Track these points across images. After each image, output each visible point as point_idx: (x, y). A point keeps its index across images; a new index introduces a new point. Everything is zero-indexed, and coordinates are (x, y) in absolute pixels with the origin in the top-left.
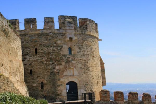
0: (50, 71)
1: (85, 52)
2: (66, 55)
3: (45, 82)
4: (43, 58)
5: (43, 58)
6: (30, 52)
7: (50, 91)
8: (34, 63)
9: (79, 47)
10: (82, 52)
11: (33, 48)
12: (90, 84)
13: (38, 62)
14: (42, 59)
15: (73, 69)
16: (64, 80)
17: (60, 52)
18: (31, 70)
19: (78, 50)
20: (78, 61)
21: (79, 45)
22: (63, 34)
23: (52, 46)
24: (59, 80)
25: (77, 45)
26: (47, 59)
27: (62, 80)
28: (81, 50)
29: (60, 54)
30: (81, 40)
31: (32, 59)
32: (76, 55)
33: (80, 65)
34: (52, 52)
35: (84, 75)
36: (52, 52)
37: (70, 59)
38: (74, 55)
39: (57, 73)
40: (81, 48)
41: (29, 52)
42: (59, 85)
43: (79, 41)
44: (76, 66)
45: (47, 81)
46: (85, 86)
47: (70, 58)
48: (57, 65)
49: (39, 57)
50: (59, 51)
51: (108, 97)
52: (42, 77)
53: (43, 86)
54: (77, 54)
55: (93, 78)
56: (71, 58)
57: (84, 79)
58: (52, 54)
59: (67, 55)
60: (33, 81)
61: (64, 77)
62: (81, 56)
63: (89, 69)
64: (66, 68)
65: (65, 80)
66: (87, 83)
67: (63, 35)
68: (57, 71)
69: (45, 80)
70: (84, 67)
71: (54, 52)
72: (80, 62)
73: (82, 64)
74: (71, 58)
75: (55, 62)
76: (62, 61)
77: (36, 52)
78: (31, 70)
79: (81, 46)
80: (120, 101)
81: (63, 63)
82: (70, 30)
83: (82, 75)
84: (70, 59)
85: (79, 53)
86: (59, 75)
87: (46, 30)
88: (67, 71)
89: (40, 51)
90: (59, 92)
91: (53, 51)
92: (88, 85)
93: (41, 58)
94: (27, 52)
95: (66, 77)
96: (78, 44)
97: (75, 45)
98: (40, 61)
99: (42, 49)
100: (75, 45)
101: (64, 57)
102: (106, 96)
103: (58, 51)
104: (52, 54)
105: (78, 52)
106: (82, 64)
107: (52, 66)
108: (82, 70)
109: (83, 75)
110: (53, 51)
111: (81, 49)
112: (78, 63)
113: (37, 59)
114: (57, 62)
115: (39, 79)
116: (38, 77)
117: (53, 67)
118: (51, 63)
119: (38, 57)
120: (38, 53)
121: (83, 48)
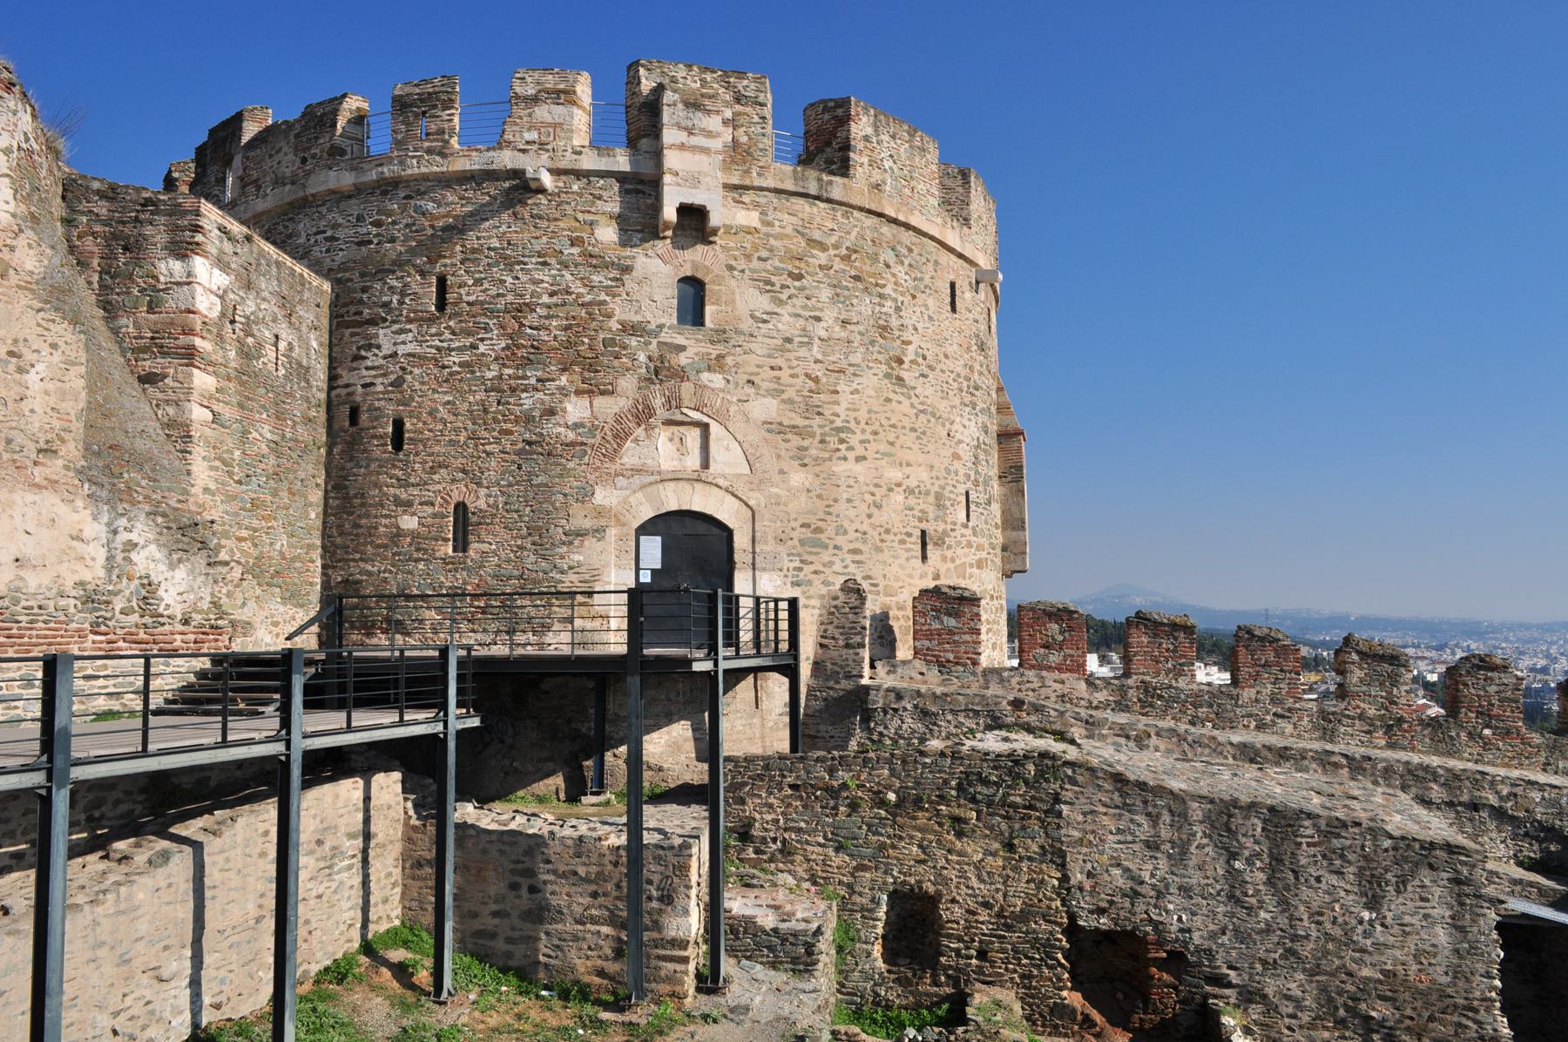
0: (520, 432)
1: (818, 319)
2: (653, 326)
3: (479, 502)
4: (482, 340)
5: (482, 340)
6: (401, 303)
7: (509, 569)
8: (416, 371)
9: (773, 285)
10: (786, 318)
11: (423, 274)
12: (840, 540)
13: (444, 367)
14: (474, 347)
15: (705, 428)
16: (625, 501)
17: (604, 303)
18: (399, 425)
19: (763, 303)
20: (756, 380)
21: (768, 265)
22: (642, 182)
23: (553, 261)
24: (585, 495)
25: (755, 264)
26: (508, 347)
27: (603, 496)
28: (781, 303)
29: (609, 316)
30: (787, 236)
31: (410, 348)
32: (738, 332)
33: (764, 408)
34: (545, 299)
35: (798, 478)
36: (545, 299)
37: (682, 356)
38: (724, 332)
39: (572, 444)
40: (783, 287)
41: (395, 299)
42: (581, 534)
43: (772, 241)
44: (733, 409)
45: (491, 501)
46: (800, 550)
47: (682, 348)
48: (578, 393)
49: (453, 333)
50: (603, 297)
51: (967, 637)
52: (464, 471)
53: (465, 533)
54: (747, 325)
55: (879, 507)
56: (691, 352)
57: (799, 505)
58: (547, 317)
59: (661, 327)
60: (404, 496)
61: (621, 481)
62: (780, 342)
63: (842, 441)
64: (643, 414)
65: (632, 500)
66: (818, 530)
67: (638, 192)
68: (571, 436)
69: (483, 492)
70: (800, 422)
71: (556, 305)
72: (765, 385)
73: (790, 401)
74: (693, 346)
75: (564, 370)
76: (616, 363)
77: (441, 304)
78: (399, 425)
79: (790, 274)
80: (1056, 675)
81: (627, 384)
82: (687, 155)
83: (777, 478)
84: (683, 359)
85: (765, 321)
86: (586, 459)
87: (515, 148)
88: (649, 437)
89: (462, 291)
90: (574, 578)
91: (551, 295)
92: (826, 547)
93: (468, 341)
94: (386, 305)
95: (637, 480)
96: (765, 260)
97: (733, 263)
98: (461, 365)
99: (478, 282)
100: (731, 268)
101: (633, 342)
102: (951, 632)
103: (588, 298)
104: (547, 317)
105: (752, 316)
106: (785, 396)
107: (540, 395)
108: (779, 437)
109: (781, 472)
110: (551, 295)
111: (784, 297)
112: (750, 390)
113: (438, 349)
114: (577, 369)
115: (439, 487)
116: (433, 471)
117: (543, 402)
118: (532, 375)
119: (447, 335)
120: (448, 311)
121: (801, 289)
